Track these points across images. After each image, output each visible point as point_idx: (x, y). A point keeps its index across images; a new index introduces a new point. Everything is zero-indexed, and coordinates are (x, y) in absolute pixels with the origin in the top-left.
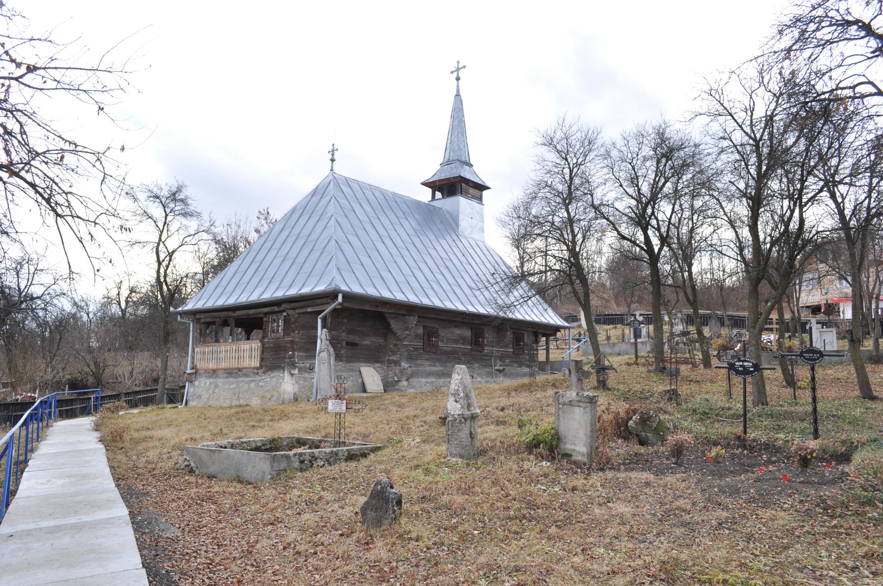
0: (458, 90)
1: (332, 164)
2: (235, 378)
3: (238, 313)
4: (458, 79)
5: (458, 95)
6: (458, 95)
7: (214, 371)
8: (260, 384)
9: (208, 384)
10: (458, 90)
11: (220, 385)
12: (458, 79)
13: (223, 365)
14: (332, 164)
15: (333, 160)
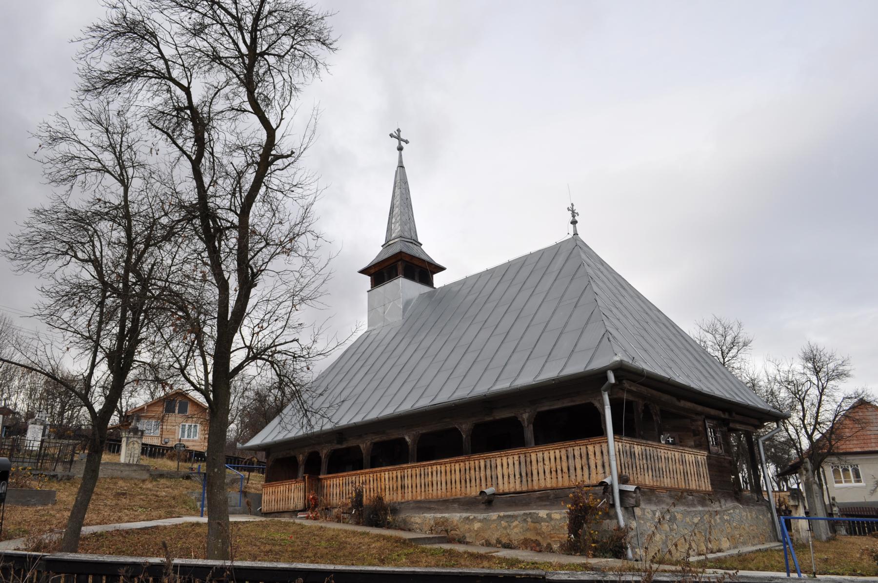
0: (401, 161)
1: (575, 227)
2: (688, 505)
3: (683, 404)
4: (400, 149)
5: (401, 166)
6: (401, 166)
7: (652, 490)
8: (726, 517)
9: (658, 514)
10: (401, 161)
11: (679, 516)
12: (400, 149)
13: (667, 482)
14: (575, 227)
15: (574, 222)
